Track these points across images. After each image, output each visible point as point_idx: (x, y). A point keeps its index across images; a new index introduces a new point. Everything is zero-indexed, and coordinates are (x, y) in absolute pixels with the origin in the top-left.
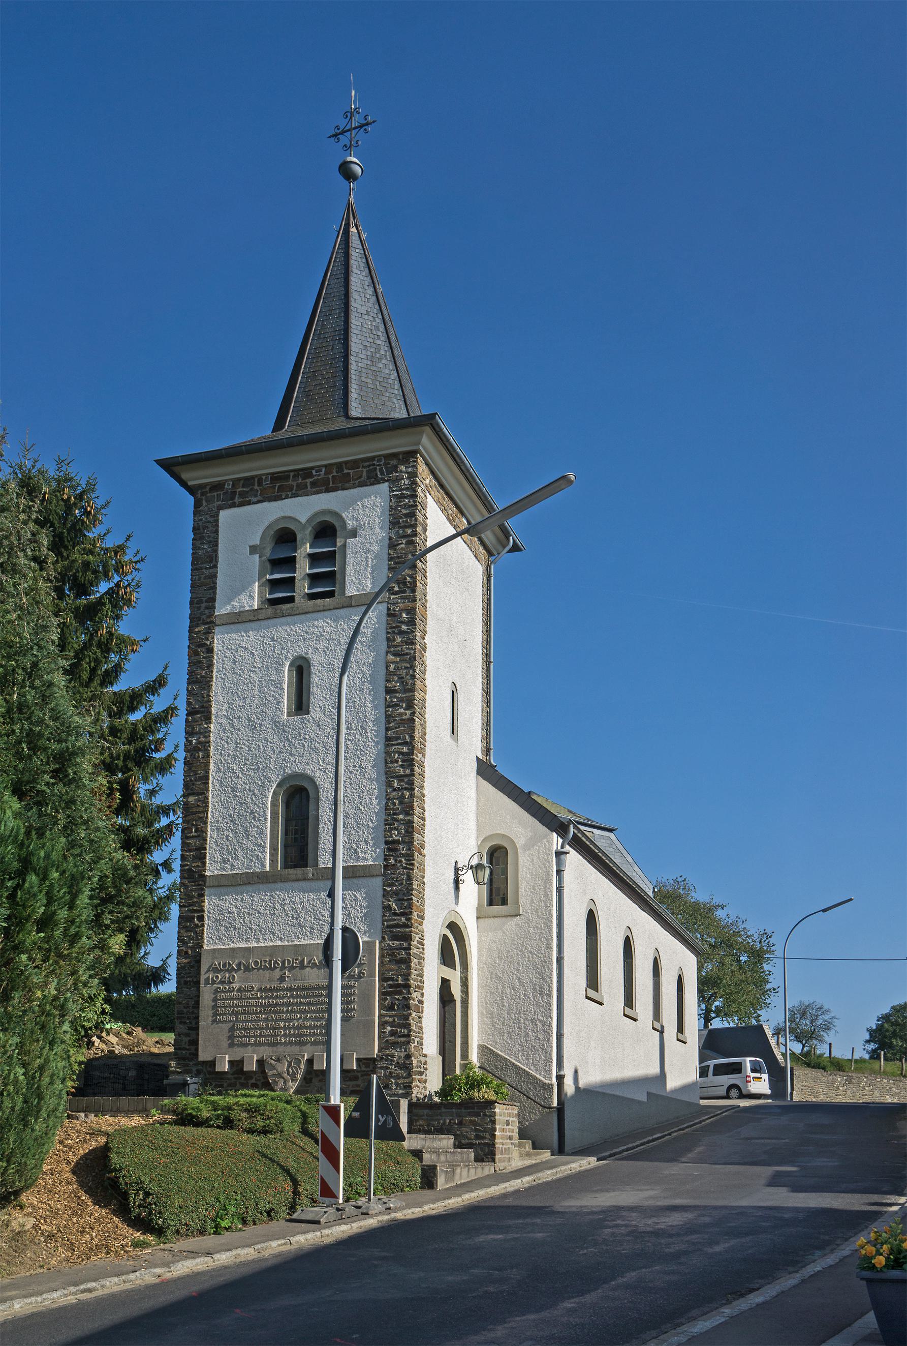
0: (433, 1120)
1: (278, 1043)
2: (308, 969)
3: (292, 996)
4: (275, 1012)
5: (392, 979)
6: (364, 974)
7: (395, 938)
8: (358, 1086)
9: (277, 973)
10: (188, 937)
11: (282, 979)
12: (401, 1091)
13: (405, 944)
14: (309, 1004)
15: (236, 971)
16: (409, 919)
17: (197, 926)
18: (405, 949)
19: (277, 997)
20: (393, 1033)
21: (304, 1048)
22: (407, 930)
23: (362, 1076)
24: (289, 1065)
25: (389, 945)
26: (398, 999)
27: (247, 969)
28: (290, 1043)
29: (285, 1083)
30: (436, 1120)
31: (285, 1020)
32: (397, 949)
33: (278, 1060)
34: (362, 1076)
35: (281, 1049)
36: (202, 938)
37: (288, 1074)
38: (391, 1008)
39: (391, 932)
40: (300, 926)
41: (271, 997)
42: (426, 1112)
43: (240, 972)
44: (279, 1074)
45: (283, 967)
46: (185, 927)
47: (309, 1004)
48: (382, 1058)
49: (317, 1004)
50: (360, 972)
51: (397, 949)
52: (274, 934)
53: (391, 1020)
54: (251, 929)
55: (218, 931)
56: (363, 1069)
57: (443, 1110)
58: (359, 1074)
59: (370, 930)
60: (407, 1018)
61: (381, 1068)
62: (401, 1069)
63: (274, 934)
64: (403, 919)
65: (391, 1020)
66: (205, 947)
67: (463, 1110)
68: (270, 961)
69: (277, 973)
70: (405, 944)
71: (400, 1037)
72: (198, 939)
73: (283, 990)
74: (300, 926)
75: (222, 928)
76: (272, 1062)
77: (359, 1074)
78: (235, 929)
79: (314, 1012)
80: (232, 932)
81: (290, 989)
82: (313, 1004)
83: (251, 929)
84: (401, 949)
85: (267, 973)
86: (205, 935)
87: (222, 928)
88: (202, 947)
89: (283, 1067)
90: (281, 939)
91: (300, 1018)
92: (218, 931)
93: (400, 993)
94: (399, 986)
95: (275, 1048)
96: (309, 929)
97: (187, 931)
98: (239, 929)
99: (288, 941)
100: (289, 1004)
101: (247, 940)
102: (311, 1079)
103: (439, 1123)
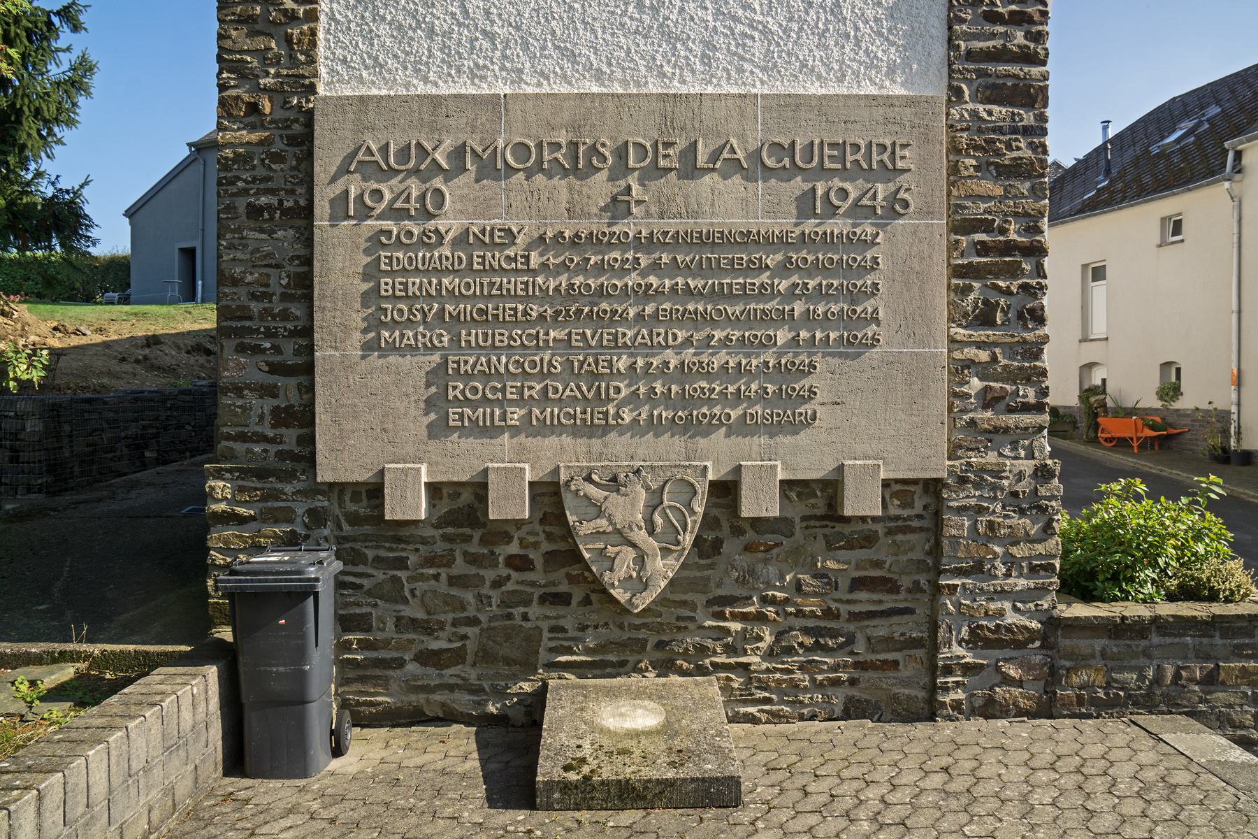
0: (1121, 669)
1: (607, 429)
2: (707, 179)
3: (655, 267)
4: (597, 319)
5: (986, 226)
6: (906, 204)
7: (994, 93)
8: (878, 564)
9: (599, 187)
10: (262, 54)
11: (618, 206)
12: (1022, 583)
13: (1028, 118)
14: (717, 295)
15: (448, 176)
16: (1039, 37)
17: (292, 17)
18: (1027, 131)
19: (600, 268)
20: (989, 400)
21: (702, 442)
22: (1035, 71)
23: (890, 532)
24: (654, 504)
25: (974, 114)
26: (1007, 292)
27: (490, 169)
28: (654, 426)
29: (641, 560)
30: (1131, 669)
31: (631, 349)
32: (1000, 130)
33: (614, 483)
34: (890, 532)
35: (618, 444)
36: (312, 61)
37: (651, 531)
38: (984, 318)
39: (982, 74)
40: (668, 36)
41: (582, 268)
42: (1099, 644)
43: (462, 180)
44: (619, 532)
45: (621, 168)
46: (246, 20)
47: (717, 295)
48: (963, 480)
49: (745, 295)
50: (893, 197)
51: (1000, 130)
52: (573, 57)
53: (984, 356)
54: (490, 36)
55: (370, 38)
56: (893, 511)
57: (1155, 639)
58: (880, 528)
59: (906, 64)
60: (1034, 351)
61: (961, 510)
62: (1022, 512)
63: (573, 57)
64: (1020, 37)
65: (984, 356)
66: (321, 90)
67: (1218, 640)
68: (574, 145)
69: (599, 187)
70: (1028, 118)
71: (1011, 410)
72: (297, 64)
73: (622, 245)
74: (668, 36)
75: (384, 30)
76: (592, 490)
77: (880, 528)
78: (431, 33)
79: (735, 322)
80: (421, 44)
81: (649, 243)
82: (731, 297)
83: (490, 36)
84: (1014, 130)
85: (561, 184)
86: (321, 50)
87: (384, 30)
88: (312, 89)
89: (629, 509)
90: (599, 76)
91: (688, 342)
92: (370, 38)
93: (1013, 271)
94: (1009, 248)
95: (596, 443)
96: (698, 49)
97: (252, 34)
98: (447, 34)
99: (624, 82)
100: (646, 294)
101: (476, 74)
102: (717, 545)
103: (1142, 678)
